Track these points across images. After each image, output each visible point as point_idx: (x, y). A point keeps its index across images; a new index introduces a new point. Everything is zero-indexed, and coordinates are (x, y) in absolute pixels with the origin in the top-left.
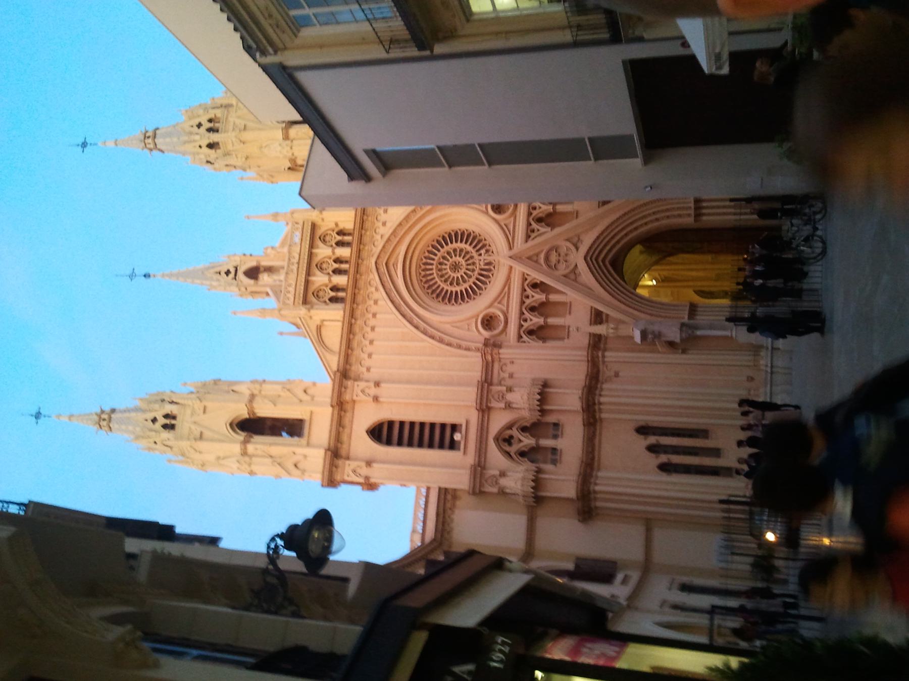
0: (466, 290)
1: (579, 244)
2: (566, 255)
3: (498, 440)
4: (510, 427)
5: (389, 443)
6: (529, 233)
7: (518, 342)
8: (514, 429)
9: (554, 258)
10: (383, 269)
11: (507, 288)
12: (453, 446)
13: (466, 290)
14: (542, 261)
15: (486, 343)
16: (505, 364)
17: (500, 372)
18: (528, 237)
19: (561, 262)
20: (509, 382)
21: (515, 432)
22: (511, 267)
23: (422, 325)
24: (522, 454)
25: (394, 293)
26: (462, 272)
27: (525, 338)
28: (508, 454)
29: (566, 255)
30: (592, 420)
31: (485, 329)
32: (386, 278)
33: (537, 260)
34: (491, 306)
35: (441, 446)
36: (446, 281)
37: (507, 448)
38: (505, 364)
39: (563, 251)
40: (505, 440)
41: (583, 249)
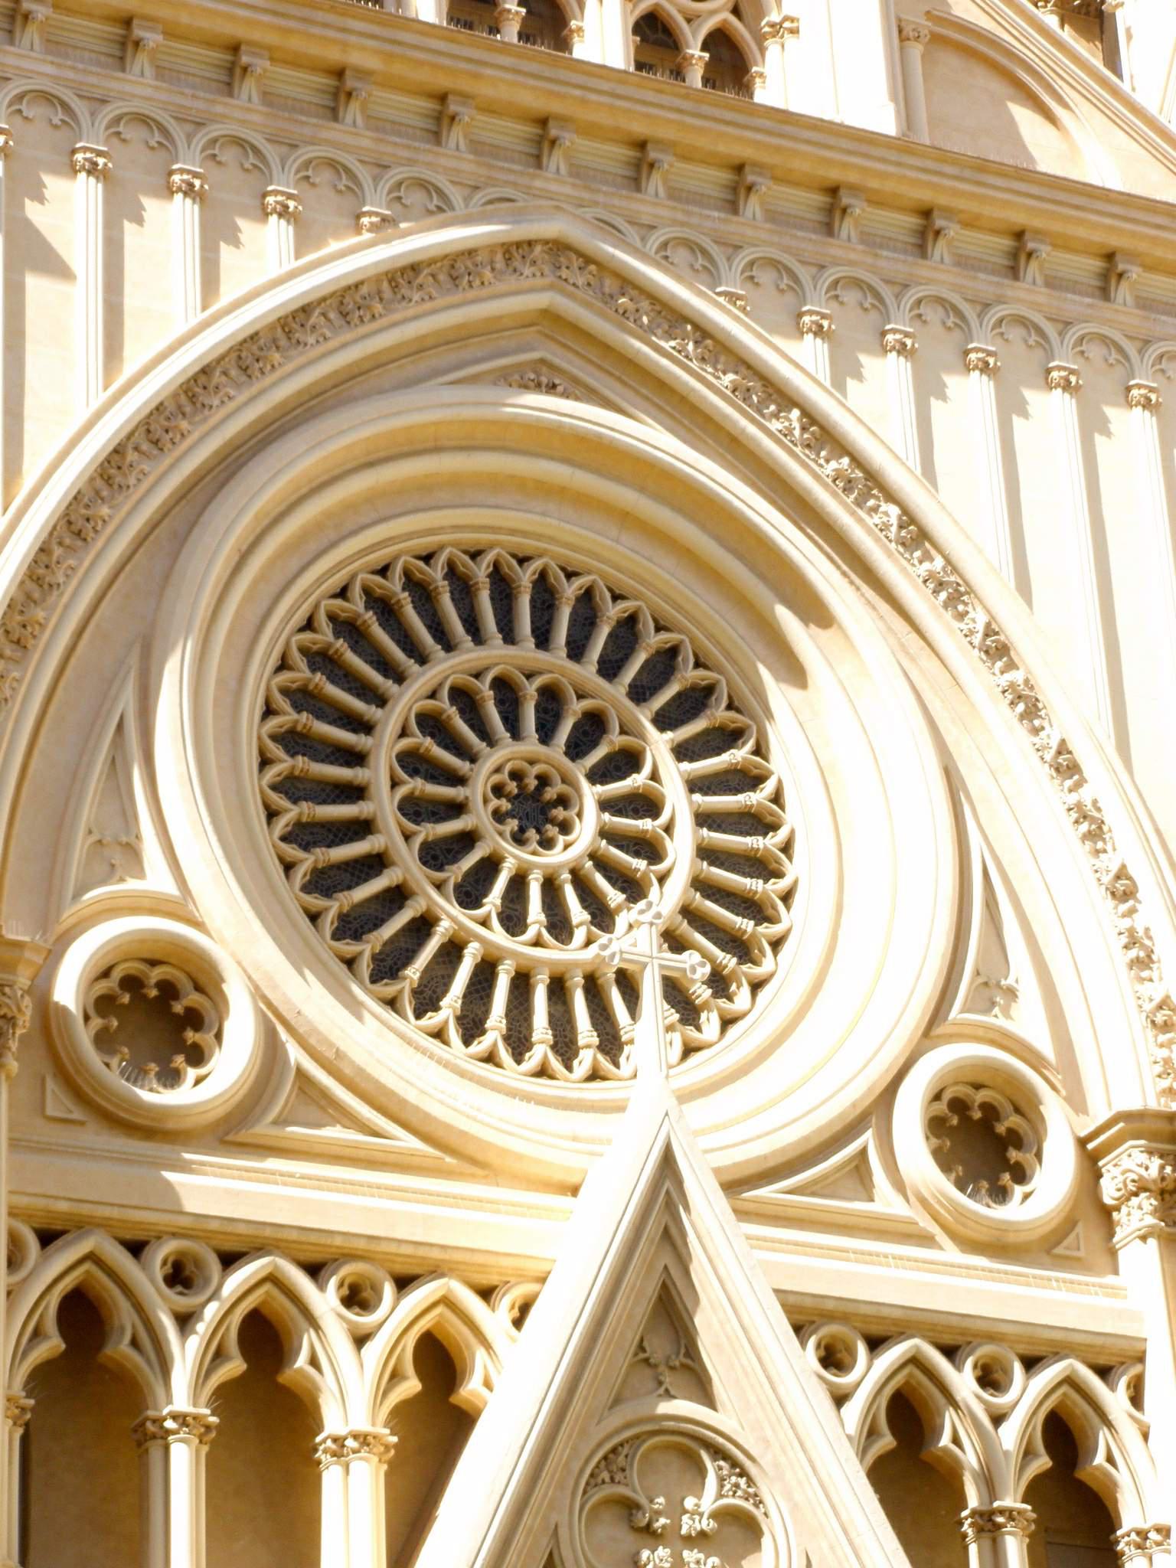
0: (377, 863)
11: (410, 1142)
13: (377, 863)
22: (574, 1191)
26: (496, 840)
36: (432, 724)
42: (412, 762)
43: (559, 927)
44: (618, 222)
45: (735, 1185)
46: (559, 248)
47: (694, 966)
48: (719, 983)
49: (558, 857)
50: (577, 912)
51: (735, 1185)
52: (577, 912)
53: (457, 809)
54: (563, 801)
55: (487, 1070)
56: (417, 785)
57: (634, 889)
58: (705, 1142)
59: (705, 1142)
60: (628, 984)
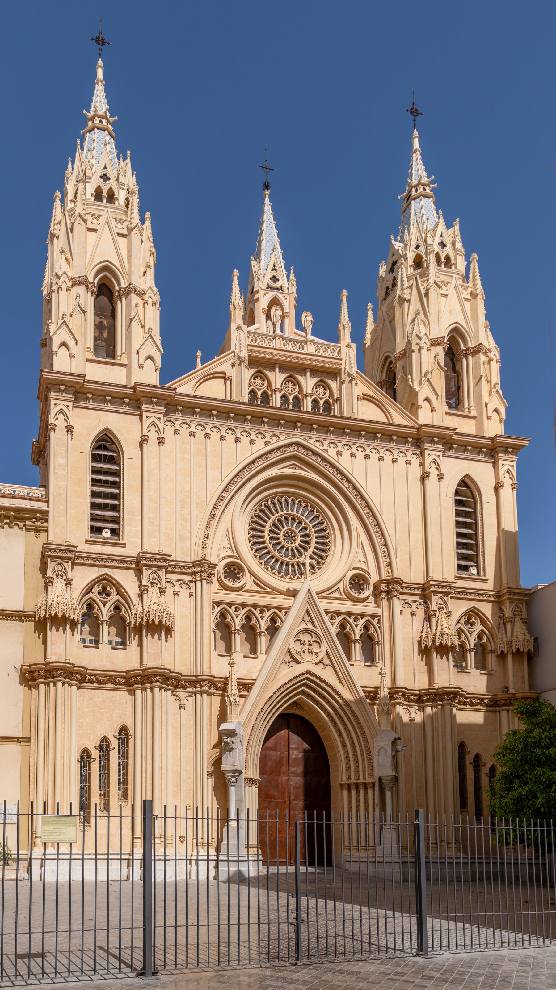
1: (322, 666)
2: (311, 652)
3: (105, 579)
4: (121, 592)
5: (95, 458)
6: (333, 614)
7: (213, 602)
8: (118, 597)
9: (306, 638)
10: (291, 451)
12: (96, 530)
14: (303, 626)
15: (212, 566)
16: (189, 587)
17: (180, 582)
18: (327, 612)
19: (302, 646)
20: (170, 591)
21: (114, 597)
23: (228, 495)
24: (90, 606)
25: (262, 464)
27: (217, 610)
28: (90, 590)
29: (311, 652)
30: (133, 680)
31: (227, 566)
32: (279, 455)
33: (304, 621)
34: (251, 573)
35: (93, 518)
37: (96, 590)
38: (189, 587)
39: (315, 648)
40: (104, 588)
41: (318, 670)
42: (271, 531)
43: (294, 556)
44: (308, 438)
45: (318, 594)
46: (297, 444)
47: (314, 562)
48: (318, 563)
49: (294, 545)
50: (296, 553)
51: (318, 594)
52: (296, 553)
53: (278, 539)
54: (294, 536)
55: (282, 579)
56: (272, 535)
57: (305, 549)
58: (314, 588)
59: (314, 588)
60: (304, 564)
